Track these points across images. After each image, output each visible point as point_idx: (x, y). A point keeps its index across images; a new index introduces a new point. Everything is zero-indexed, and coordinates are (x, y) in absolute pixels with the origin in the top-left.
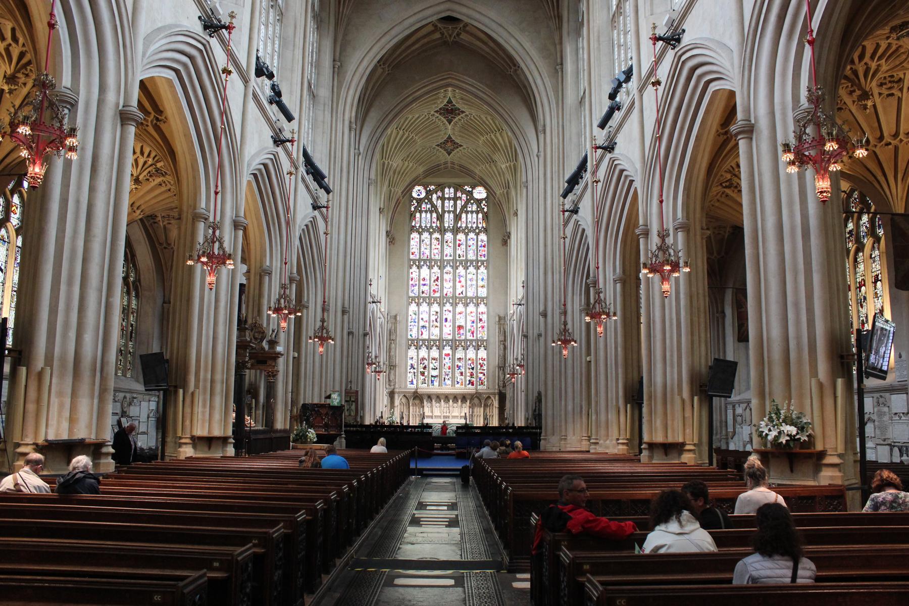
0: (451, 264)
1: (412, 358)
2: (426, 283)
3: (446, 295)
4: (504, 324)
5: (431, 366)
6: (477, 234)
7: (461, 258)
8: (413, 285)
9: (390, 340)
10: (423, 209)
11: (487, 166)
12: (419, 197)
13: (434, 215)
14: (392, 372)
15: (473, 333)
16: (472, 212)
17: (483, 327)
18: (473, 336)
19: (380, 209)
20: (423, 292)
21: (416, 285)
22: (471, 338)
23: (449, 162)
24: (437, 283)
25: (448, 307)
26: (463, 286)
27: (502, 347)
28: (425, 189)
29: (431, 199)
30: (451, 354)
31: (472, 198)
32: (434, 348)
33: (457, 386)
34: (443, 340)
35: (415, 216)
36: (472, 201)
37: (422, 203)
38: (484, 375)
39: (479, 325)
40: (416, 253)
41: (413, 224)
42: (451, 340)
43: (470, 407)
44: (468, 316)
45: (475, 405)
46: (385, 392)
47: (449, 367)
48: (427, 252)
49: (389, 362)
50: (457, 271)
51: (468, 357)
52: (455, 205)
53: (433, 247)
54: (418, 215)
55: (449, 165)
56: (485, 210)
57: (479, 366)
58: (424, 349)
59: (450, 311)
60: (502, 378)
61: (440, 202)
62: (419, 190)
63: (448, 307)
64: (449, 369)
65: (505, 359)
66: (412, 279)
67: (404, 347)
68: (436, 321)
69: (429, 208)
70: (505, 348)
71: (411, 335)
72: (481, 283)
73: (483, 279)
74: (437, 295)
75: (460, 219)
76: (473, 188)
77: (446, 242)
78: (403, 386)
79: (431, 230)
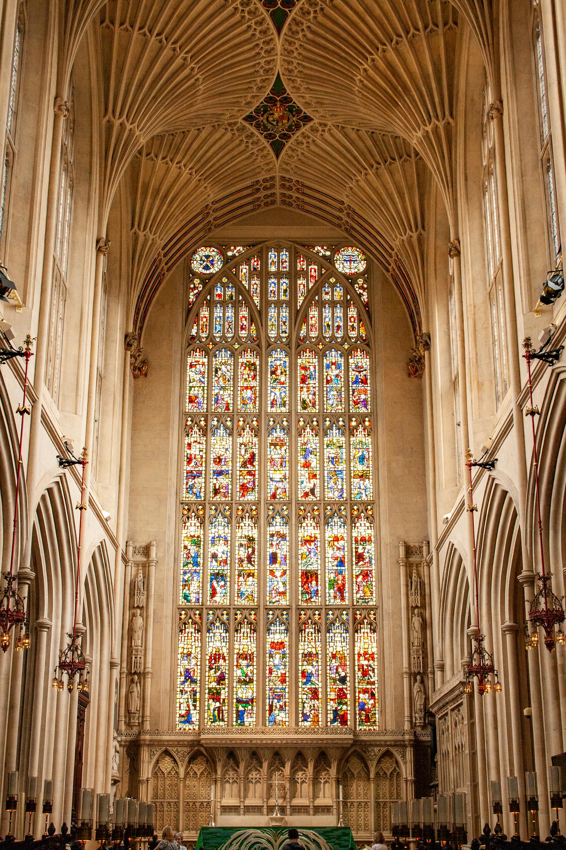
0: (285, 423)
1: (189, 655)
2: (224, 468)
3: (274, 496)
4: (418, 565)
5: (238, 673)
6: (347, 354)
7: (310, 410)
8: (192, 475)
9: (132, 607)
10: (217, 299)
11: (372, 177)
12: (208, 272)
13: (244, 312)
14: (136, 689)
15: (341, 590)
16: (333, 304)
17: (366, 575)
18: (343, 599)
19: (98, 242)
20: (216, 492)
21: (199, 474)
22: (338, 601)
23: (278, 183)
24: (250, 468)
25: (278, 526)
26: (315, 476)
27: (416, 621)
28: (222, 253)
29: (237, 275)
30: (287, 644)
31: (334, 272)
32: (245, 629)
33: (306, 724)
34: (267, 609)
35: (198, 315)
36: (332, 280)
37: (214, 286)
38: (373, 696)
39: (356, 570)
40: (200, 399)
41: (194, 332)
42: (288, 609)
43: (338, 782)
44: (330, 552)
45: (353, 774)
46: (114, 744)
47: (283, 675)
48: (227, 396)
49: (129, 663)
50: (301, 440)
51: (330, 650)
52: (293, 289)
53: (240, 384)
54: (204, 313)
55: (278, 190)
56: (365, 298)
57: (360, 674)
58: (219, 631)
59: (283, 537)
60: (419, 703)
61: (256, 281)
62: (207, 257)
63: (278, 526)
64: (283, 681)
65: (425, 657)
66: (190, 461)
67: (168, 625)
68: (250, 561)
69: (231, 297)
70: (425, 625)
71: (186, 597)
72: (360, 468)
73: (362, 459)
74: (251, 497)
75: (305, 319)
76: (335, 249)
77: (273, 373)
78: (165, 726)
79: (236, 346)
